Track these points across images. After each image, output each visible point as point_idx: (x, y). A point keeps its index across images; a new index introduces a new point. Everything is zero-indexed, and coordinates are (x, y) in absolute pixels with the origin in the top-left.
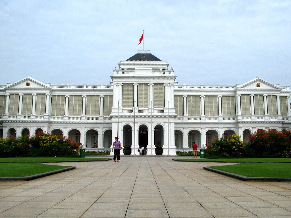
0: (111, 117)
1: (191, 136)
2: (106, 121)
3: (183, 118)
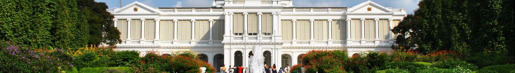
0: (223, 44)
1: (284, 60)
2: (216, 45)
3: (292, 43)
